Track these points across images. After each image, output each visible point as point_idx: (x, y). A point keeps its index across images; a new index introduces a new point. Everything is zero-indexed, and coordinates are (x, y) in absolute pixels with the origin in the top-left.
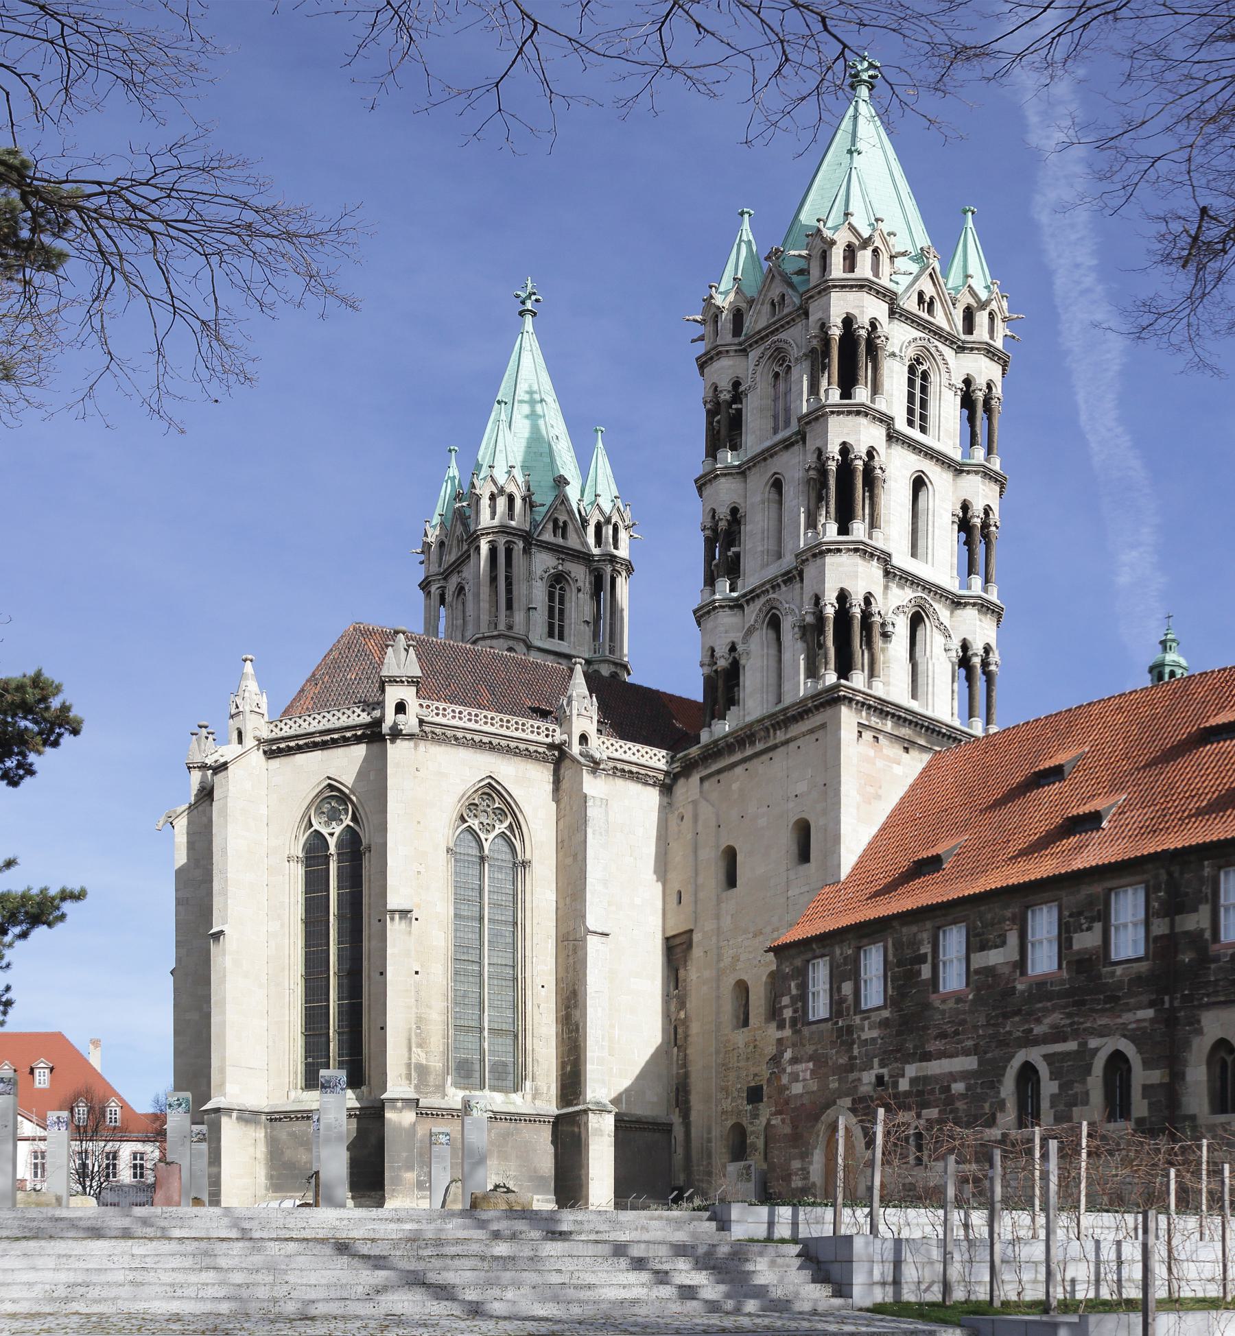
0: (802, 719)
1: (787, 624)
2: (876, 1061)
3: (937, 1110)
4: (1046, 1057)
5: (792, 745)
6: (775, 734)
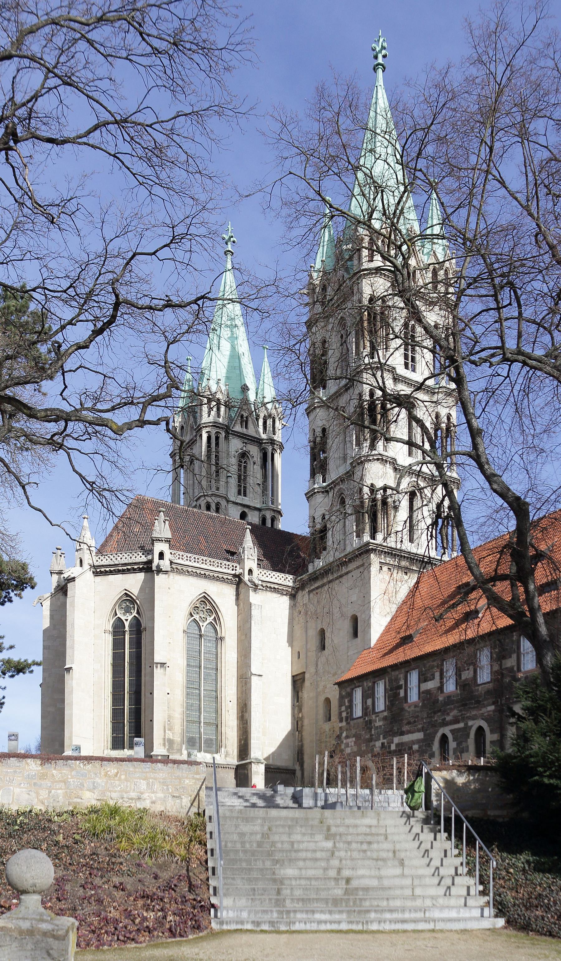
2: (381, 736)
4: (452, 731)
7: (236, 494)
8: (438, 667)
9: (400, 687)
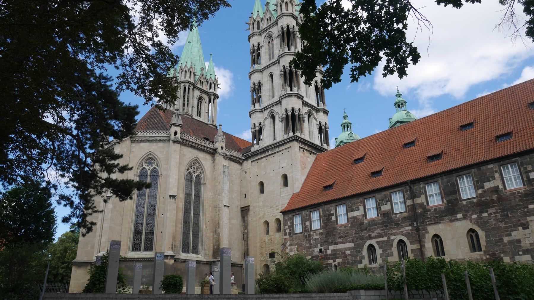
0: (284, 145)
1: (277, 118)
2: (319, 245)
3: (341, 259)
5: (281, 153)
6: (275, 149)
7: (196, 115)
8: (361, 202)
9: (332, 215)
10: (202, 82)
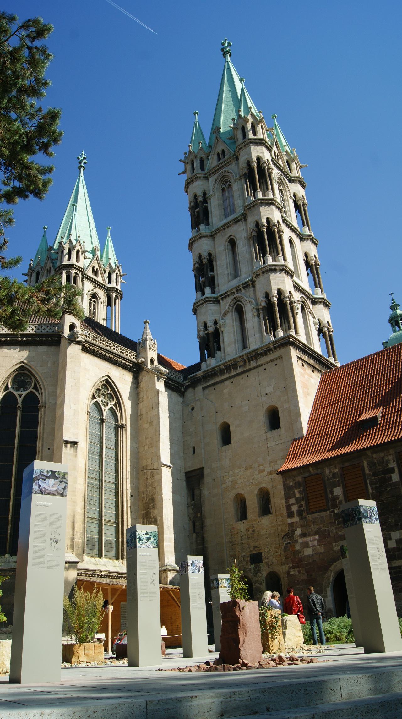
5: (261, 369)
6: (250, 363)
10: (96, 270)
